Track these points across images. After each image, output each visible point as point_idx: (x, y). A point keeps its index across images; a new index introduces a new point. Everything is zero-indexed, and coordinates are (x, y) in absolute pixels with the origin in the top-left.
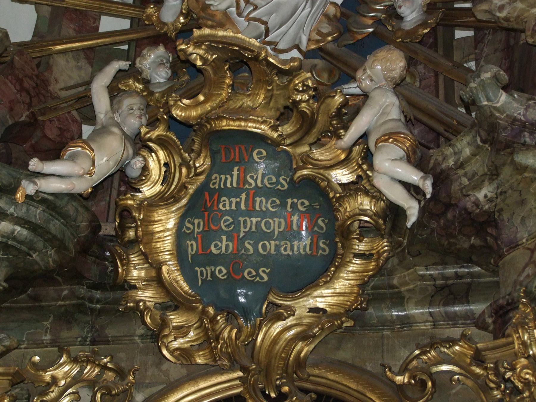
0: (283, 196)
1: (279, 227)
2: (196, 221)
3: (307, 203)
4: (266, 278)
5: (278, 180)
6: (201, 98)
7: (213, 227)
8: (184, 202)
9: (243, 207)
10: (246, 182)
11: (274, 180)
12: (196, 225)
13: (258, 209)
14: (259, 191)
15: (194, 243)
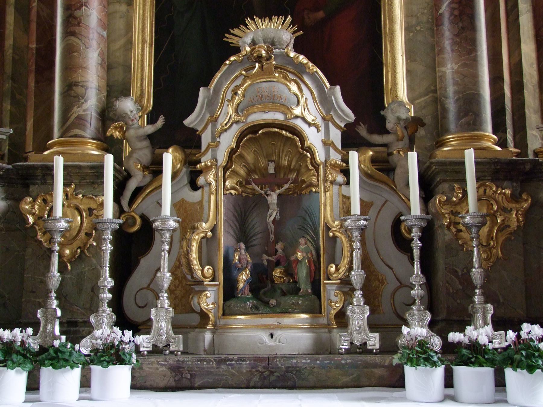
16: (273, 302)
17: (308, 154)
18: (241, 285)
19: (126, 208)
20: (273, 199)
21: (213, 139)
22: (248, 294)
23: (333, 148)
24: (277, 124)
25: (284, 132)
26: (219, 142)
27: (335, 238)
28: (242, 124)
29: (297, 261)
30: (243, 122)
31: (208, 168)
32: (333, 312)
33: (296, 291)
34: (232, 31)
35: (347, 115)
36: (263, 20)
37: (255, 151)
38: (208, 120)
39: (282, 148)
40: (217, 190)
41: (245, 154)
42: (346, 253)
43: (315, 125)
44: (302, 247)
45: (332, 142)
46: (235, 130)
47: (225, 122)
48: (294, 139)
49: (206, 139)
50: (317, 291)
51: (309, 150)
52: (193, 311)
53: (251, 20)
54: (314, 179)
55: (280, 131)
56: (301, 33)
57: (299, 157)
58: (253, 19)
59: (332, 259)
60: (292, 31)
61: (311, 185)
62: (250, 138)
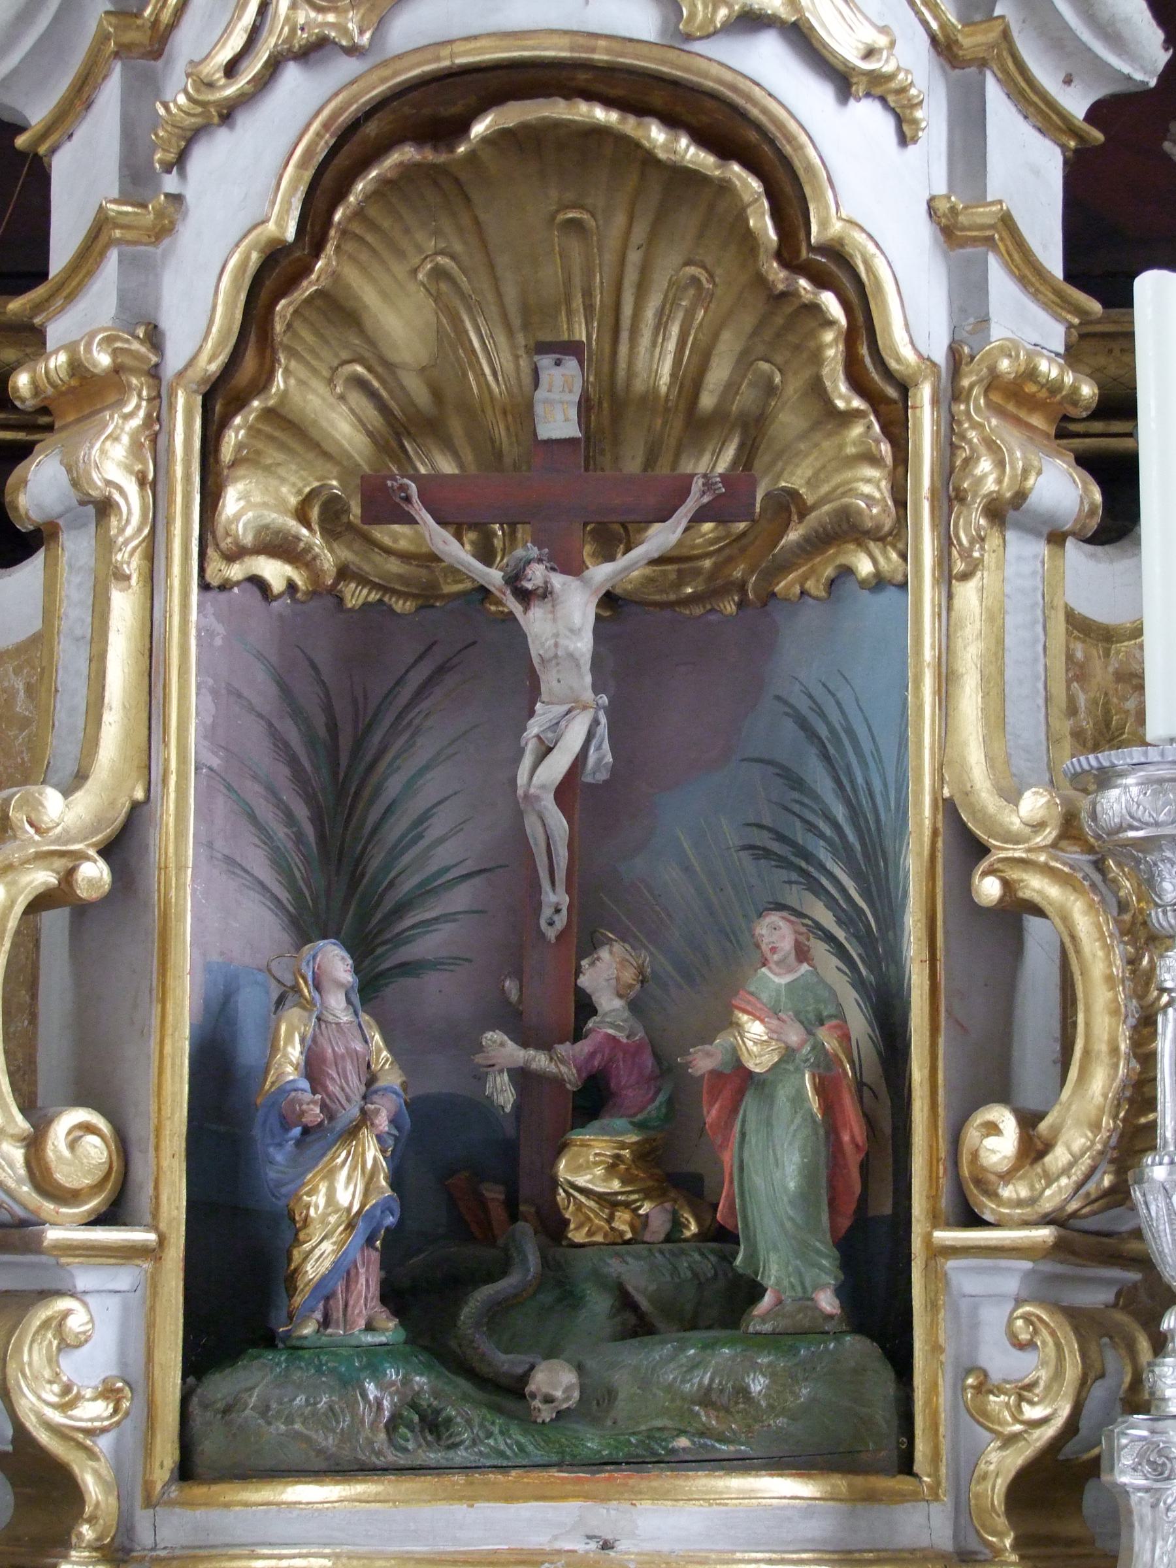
16: (555, 1381)
17: (830, 301)
18: (319, 1256)
20: (564, 623)
21: (136, 177)
22: (368, 1321)
23: (1010, 267)
24: (610, 71)
25: (656, 135)
26: (177, 199)
27: (1015, 911)
28: (346, 68)
29: (739, 1081)
30: (353, 50)
31: (89, 393)
32: (1001, 1465)
33: (727, 1300)
35: (1113, 36)
37: (439, 273)
38: (103, 38)
39: (634, 257)
40: (152, 552)
41: (369, 296)
42: (1103, 1021)
43: (883, 89)
44: (775, 979)
45: (1007, 221)
46: (297, 110)
47: (225, 55)
48: (724, 188)
49: (81, 182)
50: (879, 1303)
51: (838, 267)
54: (870, 488)
55: (629, 125)
57: (756, 332)
59: (990, 1077)
61: (847, 529)
62: (409, 171)
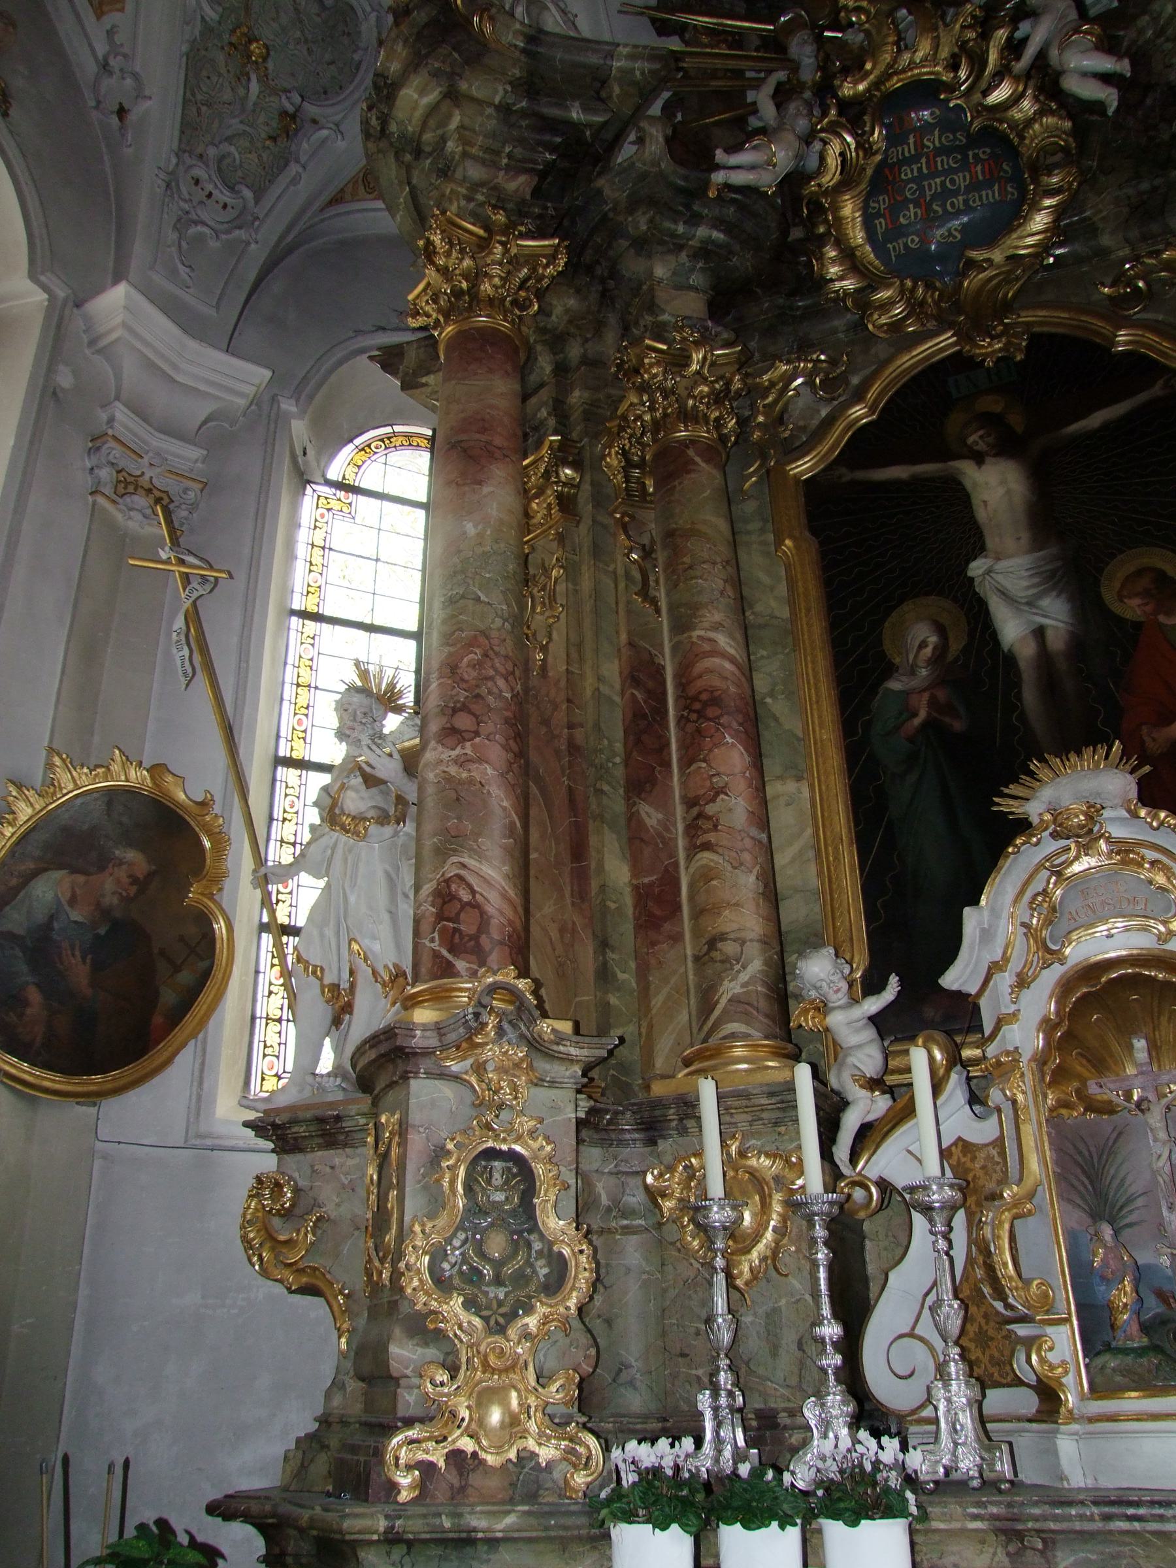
0: (962, 150)
1: (965, 180)
2: (881, 198)
3: (988, 151)
4: (959, 237)
5: (954, 136)
6: (868, 66)
7: (899, 198)
8: (863, 186)
9: (925, 171)
10: (923, 146)
11: (951, 137)
12: (882, 203)
13: (940, 168)
14: (939, 151)
15: (882, 220)
19: (846, 1170)
34: (1006, 791)
36: (1064, 758)
52: (1018, 1382)
53: (1039, 762)
56: (1147, 769)
58: (1042, 760)
60: (1128, 767)
62: (1085, 996)
